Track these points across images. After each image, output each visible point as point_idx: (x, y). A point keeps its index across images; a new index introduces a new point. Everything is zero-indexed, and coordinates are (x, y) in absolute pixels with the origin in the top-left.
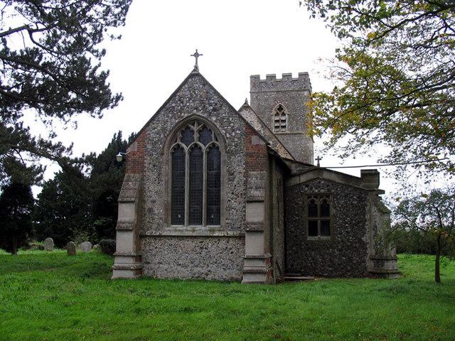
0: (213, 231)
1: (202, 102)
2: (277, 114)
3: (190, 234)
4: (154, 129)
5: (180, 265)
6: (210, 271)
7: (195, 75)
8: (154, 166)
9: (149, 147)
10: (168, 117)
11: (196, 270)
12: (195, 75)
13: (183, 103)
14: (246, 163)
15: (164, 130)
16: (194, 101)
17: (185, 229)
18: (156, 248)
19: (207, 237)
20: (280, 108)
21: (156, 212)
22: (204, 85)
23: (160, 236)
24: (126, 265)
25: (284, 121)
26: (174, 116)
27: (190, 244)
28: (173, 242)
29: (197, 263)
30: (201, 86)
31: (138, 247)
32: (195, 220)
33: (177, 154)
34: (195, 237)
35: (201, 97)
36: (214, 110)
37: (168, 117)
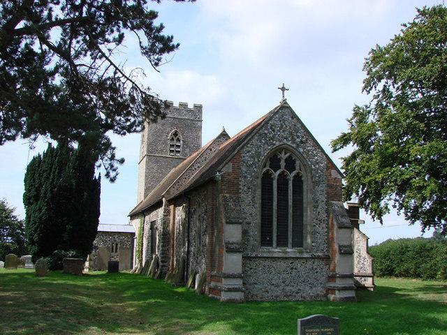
0: (301, 252)
1: (291, 134)
2: (172, 139)
3: (281, 255)
4: (249, 152)
5: (273, 285)
6: (299, 290)
7: (284, 107)
8: (249, 189)
9: (244, 169)
10: (261, 142)
11: (288, 289)
12: (284, 107)
13: (273, 131)
14: (327, 193)
15: (258, 155)
16: (283, 131)
17: (277, 251)
18: (251, 269)
19: (297, 258)
20: (175, 134)
21: (251, 233)
22: (292, 118)
23: (256, 257)
24: (236, 286)
25: (179, 146)
26: (266, 143)
27: (282, 265)
28: (267, 263)
29: (287, 282)
30: (290, 119)
31: (244, 265)
32: (282, 242)
33: (267, 179)
34: (286, 258)
35: (290, 128)
36: (302, 142)
37: (261, 142)
